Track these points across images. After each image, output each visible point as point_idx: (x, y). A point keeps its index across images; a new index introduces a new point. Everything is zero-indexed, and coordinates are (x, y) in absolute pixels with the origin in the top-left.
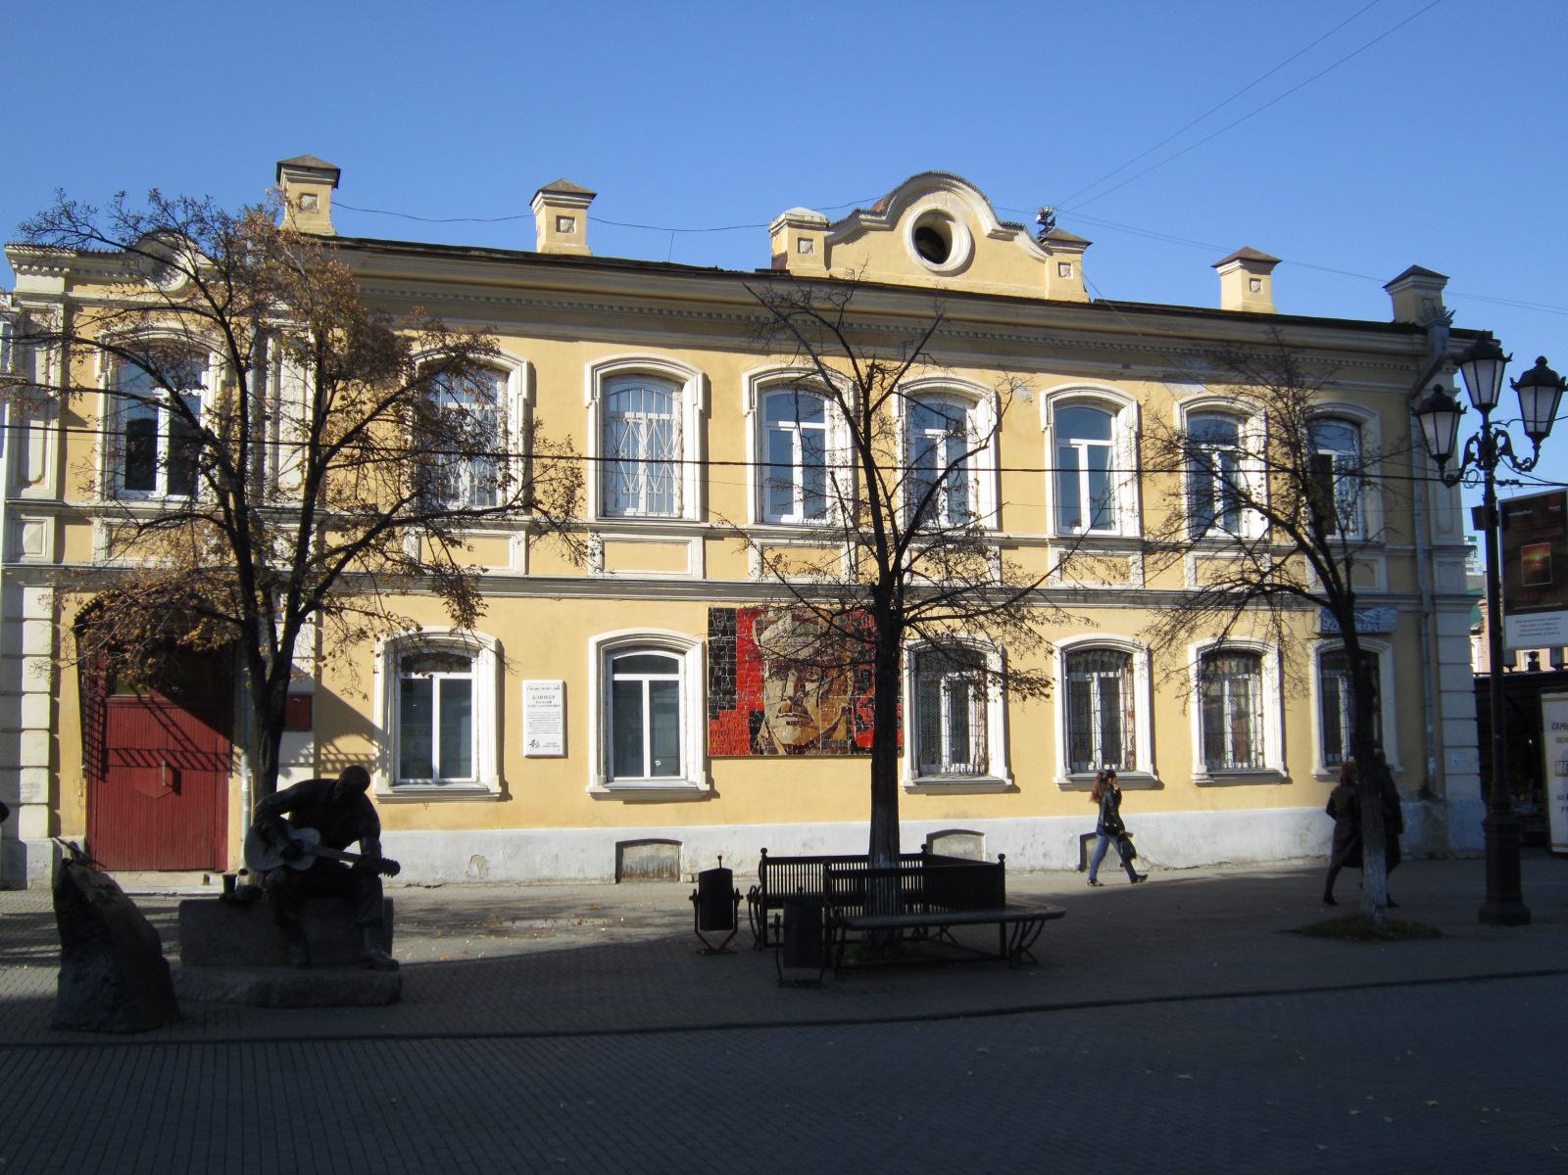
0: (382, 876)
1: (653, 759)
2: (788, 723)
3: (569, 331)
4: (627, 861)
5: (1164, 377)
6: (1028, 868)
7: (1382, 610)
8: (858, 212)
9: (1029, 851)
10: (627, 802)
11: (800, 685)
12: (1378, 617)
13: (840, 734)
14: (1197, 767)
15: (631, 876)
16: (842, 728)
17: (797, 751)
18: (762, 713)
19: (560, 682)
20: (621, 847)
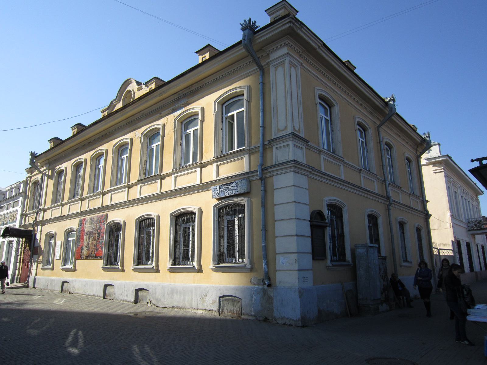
1: (71, 261)
3: (70, 158)
4: (64, 287)
5: (172, 111)
8: (112, 102)
9: (123, 293)
12: (237, 186)
14: (169, 265)
17: (87, 258)
19: (60, 242)
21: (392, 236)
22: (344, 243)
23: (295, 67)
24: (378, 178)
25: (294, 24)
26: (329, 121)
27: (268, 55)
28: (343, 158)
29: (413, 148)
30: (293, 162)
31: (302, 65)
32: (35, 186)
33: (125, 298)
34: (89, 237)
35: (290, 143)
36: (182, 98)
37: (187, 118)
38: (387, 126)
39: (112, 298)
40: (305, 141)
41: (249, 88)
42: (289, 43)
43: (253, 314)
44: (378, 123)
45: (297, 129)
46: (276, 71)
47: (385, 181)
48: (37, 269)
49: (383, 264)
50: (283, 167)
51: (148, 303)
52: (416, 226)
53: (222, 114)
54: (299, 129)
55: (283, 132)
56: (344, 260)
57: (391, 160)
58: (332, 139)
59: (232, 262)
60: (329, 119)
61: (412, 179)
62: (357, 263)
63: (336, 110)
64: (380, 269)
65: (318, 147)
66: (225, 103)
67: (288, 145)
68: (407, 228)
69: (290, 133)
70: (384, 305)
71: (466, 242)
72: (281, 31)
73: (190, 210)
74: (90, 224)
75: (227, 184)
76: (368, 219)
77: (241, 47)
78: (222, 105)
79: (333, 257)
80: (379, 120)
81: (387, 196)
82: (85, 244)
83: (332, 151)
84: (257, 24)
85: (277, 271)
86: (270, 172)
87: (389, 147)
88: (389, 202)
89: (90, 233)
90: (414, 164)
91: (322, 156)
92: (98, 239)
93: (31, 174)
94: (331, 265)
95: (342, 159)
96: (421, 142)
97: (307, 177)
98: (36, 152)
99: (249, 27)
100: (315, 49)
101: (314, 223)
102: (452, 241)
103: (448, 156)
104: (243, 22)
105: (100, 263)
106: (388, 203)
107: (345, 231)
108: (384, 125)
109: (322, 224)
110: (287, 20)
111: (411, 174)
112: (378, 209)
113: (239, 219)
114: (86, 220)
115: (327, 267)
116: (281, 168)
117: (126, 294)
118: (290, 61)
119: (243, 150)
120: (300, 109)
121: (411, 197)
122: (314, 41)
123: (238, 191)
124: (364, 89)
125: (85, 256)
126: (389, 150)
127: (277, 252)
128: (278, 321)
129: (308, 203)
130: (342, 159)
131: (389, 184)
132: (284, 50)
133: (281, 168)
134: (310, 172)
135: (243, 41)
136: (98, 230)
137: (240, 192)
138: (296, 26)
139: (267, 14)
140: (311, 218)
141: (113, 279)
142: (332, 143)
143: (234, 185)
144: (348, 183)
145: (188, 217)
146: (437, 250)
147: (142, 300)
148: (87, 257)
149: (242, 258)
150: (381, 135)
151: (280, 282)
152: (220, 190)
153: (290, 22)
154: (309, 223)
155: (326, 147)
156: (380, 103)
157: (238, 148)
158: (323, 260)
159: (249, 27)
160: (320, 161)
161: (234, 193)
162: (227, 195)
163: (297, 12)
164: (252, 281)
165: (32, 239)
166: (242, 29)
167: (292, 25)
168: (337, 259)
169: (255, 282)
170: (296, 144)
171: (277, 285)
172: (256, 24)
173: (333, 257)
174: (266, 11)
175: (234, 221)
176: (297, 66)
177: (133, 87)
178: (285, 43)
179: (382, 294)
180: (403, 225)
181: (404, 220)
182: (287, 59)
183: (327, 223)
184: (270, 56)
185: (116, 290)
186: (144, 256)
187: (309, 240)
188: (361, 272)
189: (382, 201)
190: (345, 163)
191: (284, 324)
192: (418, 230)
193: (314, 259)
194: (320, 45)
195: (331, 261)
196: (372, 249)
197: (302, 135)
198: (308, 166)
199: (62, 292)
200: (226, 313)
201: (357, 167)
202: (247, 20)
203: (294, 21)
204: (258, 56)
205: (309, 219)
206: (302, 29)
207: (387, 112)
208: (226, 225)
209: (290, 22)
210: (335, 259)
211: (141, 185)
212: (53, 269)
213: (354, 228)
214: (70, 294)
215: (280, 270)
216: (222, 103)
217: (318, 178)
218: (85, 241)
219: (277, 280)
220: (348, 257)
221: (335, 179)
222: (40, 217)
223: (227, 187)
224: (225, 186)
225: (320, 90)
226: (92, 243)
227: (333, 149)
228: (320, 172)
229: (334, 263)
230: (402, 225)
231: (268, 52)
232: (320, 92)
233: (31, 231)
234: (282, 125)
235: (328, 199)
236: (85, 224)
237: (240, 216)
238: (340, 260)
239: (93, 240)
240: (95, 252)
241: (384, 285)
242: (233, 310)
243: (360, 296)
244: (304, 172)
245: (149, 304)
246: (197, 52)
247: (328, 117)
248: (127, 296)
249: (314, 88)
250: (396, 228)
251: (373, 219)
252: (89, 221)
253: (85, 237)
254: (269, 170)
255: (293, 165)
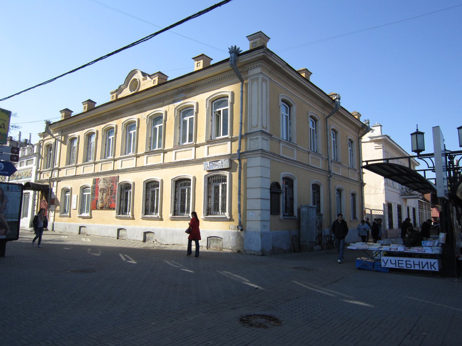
0: (189, 234)
1: (86, 210)
2: (101, 202)
3: (82, 128)
4: (81, 231)
5: (173, 102)
6: (133, 240)
7: (223, 160)
8: (120, 86)
9: (134, 235)
10: (82, 218)
11: (103, 194)
12: (222, 163)
13: (107, 205)
14: (171, 215)
15: (83, 234)
16: (108, 203)
17: (102, 208)
18: (98, 200)
19: (76, 195)
20: (80, 227)
21: (330, 199)
22: (293, 204)
23: (266, 81)
24: (322, 157)
25: (266, 53)
26: (289, 117)
27: (247, 71)
28: (297, 145)
29: (356, 131)
30: (261, 151)
31: (270, 79)
32: (48, 148)
33: (136, 238)
34: (103, 193)
35: (260, 137)
36: (181, 92)
37: (184, 109)
38: (335, 117)
39: (125, 238)
40: (270, 135)
41: (233, 94)
42: (262, 65)
43: (230, 248)
44: (327, 114)
45: (265, 127)
46: (252, 83)
47: (328, 159)
48: (54, 216)
49: (319, 219)
50: (254, 153)
51: (154, 242)
52: (352, 191)
53: (212, 109)
54: (266, 127)
55: (255, 129)
56: (293, 215)
57: (335, 142)
58: (290, 130)
59: (217, 214)
60: (288, 115)
61: (352, 156)
62: (301, 217)
63: (294, 109)
64: (317, 222)
65: (278, 138)
66: (214, 101)
67: (257, 138)
68: (344, 194)
69: (260, 131)
70: (318, 246)
71: (398, 205)
72: (256, 57)
73: (187, 177)
74: (103, 183)
75: (215, 161)
76: (312, 187)
77: (228, 63)
78: (212, 102)
79: (284, 213)
80: (329, 112)
81: (329, 170)
82: (100, 197)
83: (289, 141)
84: (240, 49)
85: (247, 221)
86: (245, 155)
87: (335, 132)
88: (330, 175)
89: (103, 190)
90: (355, 144)
91: (281, 144)
92: (111, 195)
93: (44, 138)
94: (282, 218)
95: (296, 145)
96: (362, 127)
97: (269, 160)
98: (50, 121)
99: (235, 52)
100: (280, 68)
101: (273, 191)
102: (384, 204)
103: (386, 135)
104: (231, 47)
105: (114, 213)
106: (329, 175)
107: (294, 196)
108: (332, 116)
109: (278, 191)
110: (261, 50)
111: (352, 151)
112: (321, 180)
113: (222, 185)
114: (99, 180)
115: (280, 219)
116: (252, 153)
117: (136, 235)
118: (262, 78)
119: (227, 138)
120: (267, 112)
121: (349, 170)
122: (280, 63)
123: (222, 167)
124: (316, 91)
125: (100, 207)
126: (335, 134)
127: (247, 209)
128: (246, 252)
129: (270, 178)
130: (296, 145)
131: (331, 161)
132: (258, 70)
133: (252, 153)
134: (272, 157)
135: (230, 60)
136: (111, 189)
137: (224, 167)
138: (268, 54)
139: (248, 39)
140: (271, 187)
141: (125, 225)
142: (290, 133)
143: (220, 162)
144: (299, 162)
145: (185, 182)
146: (370, 210)
147: (149, 240)
148: (102, 208)
149: (224, 212)
150: (328, 124)
151: (249, 228)
152: (210, 165)
153: (264, 52)
154: (269, 191)
155: (285, 138)
156: (328, 101)
157: (223, 135)
158: (278, 215)
159: (235, 52)
160: (280, 148)
161: (219, 168)
162: (215, 169)
163: (270, 38)
164: (230, 227)
165: (48, 192)
166: (229, 52)
167: (265, 54)
168: (288, 214)
169: (232, 228)
170: (263, 137)
171: (247, 230)
172: (240, 49)
173: (284, 213)
174: (247, 37)
175: (218, 187)
176: (267, 81)
177: (138, 76)
178: (259, 65)
179: (317, 239)
180: (341, 191)
181: (341, 188)
182: (261, 76)
183: (282, 190)
184: (249, 71)
185: (128, 232)
186: (150, 208)
187: (269, 201)
188: (303, 224)
189: (324, 174)
190: (298, 148)
191: (251, 254)
192: (353, 195)
193: (271, 214)
194: (284, 65)
195: (283, 216)
196: (312, 209)
197: (268, 131)
198: (271, 153)
199: (79, 234)
200: (212, 248)
201: (306, 150)
202: (234, 46)
203: (266, 51)
204: (240, 71)
205: (270, 188)
206: (272, 56)
207: (334, 107)
208: (213, 189)
209: (264, 52)
210: (286, 215)
211: (147, 156)
212: (70, 217)
213: (302, 194)
214: (87, 235)
215: (249, 221)
216: (212, 101)
217: (277, 160)
218: (99, 196)
219: (247, 226)
220: (296, 213)
221: (289, 160)
222: (55, 174)
223: (215, 163)
224: (213, 163)
225: (283, 96)
226: (106, 198)
227: (290, 137)
228: (279, 156)
229: (285, 217)
230: (339, 191)
231: (247, 69)
232: (283, 98)
233: (47, 186)
234: (254, 123)
235: (283, 174)
236: (99, 182)
237: (223, 183)
238: (290, 215)
239: (106, 195)
240: (108, 204)
241: (319, 233)
242: (217, 246)
243: (301, 240)
244: (268, 157)
245: (155, 242)
246: (193, 59)
247: (288, 114)
248: (137, 236)
249: (279, 95)
250: (334, 194)
251: (316, 188)
252: (102, 180)
253: (99, 193)
254: (244, 154)
255: (261, 152)
